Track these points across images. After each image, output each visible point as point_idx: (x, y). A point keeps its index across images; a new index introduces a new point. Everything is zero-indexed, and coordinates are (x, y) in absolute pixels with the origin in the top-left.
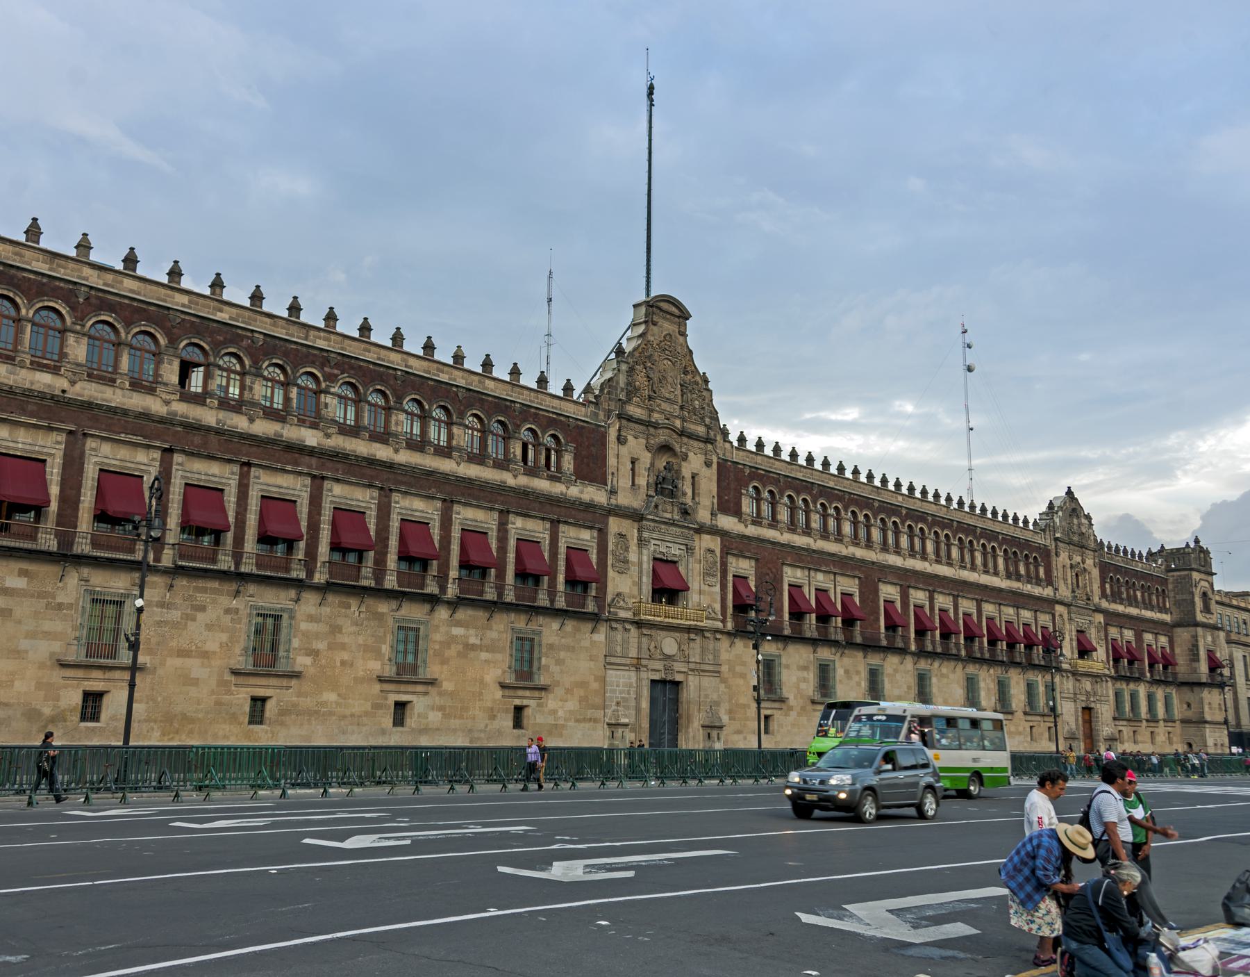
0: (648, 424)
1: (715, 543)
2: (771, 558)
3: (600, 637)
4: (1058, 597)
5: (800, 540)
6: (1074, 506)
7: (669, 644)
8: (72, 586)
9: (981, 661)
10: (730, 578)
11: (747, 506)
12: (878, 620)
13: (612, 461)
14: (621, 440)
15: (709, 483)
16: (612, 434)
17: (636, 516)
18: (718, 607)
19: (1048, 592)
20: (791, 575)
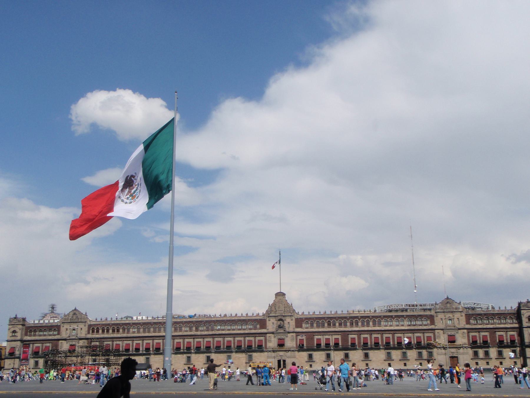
0: (275, 316)
1: (294, 334)
2: (310, 335)
3: (266, 353)
4: (436, 328)
5: (321, 330)
6: (448, 301)
7: (281, 353)
8: (185, 355)
9: (394, 348)
10: (298, 340)
11: (304, 325)
12: (348, 342)
13: (268, 324)
14: (269, 320)
15: (293, 323)
16: (268, 319)
17: (273, 333)
18: (295, 346)
19: (432, 327)
20: (316, 337)
